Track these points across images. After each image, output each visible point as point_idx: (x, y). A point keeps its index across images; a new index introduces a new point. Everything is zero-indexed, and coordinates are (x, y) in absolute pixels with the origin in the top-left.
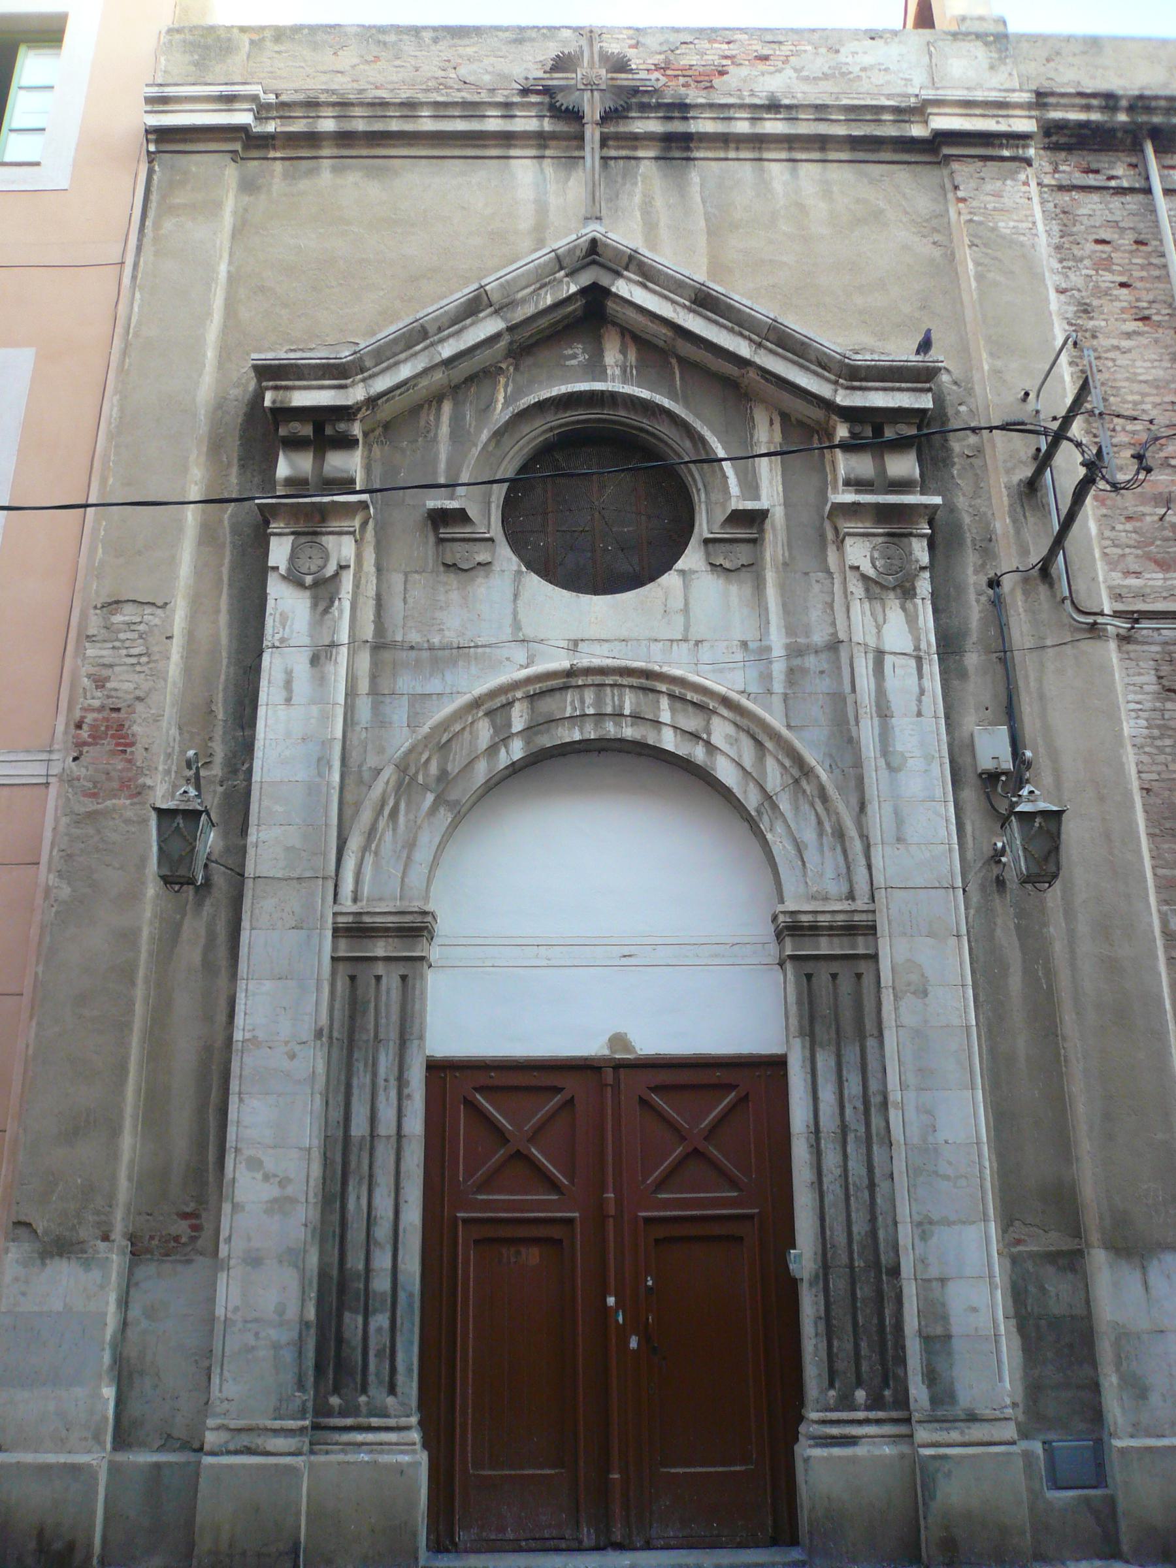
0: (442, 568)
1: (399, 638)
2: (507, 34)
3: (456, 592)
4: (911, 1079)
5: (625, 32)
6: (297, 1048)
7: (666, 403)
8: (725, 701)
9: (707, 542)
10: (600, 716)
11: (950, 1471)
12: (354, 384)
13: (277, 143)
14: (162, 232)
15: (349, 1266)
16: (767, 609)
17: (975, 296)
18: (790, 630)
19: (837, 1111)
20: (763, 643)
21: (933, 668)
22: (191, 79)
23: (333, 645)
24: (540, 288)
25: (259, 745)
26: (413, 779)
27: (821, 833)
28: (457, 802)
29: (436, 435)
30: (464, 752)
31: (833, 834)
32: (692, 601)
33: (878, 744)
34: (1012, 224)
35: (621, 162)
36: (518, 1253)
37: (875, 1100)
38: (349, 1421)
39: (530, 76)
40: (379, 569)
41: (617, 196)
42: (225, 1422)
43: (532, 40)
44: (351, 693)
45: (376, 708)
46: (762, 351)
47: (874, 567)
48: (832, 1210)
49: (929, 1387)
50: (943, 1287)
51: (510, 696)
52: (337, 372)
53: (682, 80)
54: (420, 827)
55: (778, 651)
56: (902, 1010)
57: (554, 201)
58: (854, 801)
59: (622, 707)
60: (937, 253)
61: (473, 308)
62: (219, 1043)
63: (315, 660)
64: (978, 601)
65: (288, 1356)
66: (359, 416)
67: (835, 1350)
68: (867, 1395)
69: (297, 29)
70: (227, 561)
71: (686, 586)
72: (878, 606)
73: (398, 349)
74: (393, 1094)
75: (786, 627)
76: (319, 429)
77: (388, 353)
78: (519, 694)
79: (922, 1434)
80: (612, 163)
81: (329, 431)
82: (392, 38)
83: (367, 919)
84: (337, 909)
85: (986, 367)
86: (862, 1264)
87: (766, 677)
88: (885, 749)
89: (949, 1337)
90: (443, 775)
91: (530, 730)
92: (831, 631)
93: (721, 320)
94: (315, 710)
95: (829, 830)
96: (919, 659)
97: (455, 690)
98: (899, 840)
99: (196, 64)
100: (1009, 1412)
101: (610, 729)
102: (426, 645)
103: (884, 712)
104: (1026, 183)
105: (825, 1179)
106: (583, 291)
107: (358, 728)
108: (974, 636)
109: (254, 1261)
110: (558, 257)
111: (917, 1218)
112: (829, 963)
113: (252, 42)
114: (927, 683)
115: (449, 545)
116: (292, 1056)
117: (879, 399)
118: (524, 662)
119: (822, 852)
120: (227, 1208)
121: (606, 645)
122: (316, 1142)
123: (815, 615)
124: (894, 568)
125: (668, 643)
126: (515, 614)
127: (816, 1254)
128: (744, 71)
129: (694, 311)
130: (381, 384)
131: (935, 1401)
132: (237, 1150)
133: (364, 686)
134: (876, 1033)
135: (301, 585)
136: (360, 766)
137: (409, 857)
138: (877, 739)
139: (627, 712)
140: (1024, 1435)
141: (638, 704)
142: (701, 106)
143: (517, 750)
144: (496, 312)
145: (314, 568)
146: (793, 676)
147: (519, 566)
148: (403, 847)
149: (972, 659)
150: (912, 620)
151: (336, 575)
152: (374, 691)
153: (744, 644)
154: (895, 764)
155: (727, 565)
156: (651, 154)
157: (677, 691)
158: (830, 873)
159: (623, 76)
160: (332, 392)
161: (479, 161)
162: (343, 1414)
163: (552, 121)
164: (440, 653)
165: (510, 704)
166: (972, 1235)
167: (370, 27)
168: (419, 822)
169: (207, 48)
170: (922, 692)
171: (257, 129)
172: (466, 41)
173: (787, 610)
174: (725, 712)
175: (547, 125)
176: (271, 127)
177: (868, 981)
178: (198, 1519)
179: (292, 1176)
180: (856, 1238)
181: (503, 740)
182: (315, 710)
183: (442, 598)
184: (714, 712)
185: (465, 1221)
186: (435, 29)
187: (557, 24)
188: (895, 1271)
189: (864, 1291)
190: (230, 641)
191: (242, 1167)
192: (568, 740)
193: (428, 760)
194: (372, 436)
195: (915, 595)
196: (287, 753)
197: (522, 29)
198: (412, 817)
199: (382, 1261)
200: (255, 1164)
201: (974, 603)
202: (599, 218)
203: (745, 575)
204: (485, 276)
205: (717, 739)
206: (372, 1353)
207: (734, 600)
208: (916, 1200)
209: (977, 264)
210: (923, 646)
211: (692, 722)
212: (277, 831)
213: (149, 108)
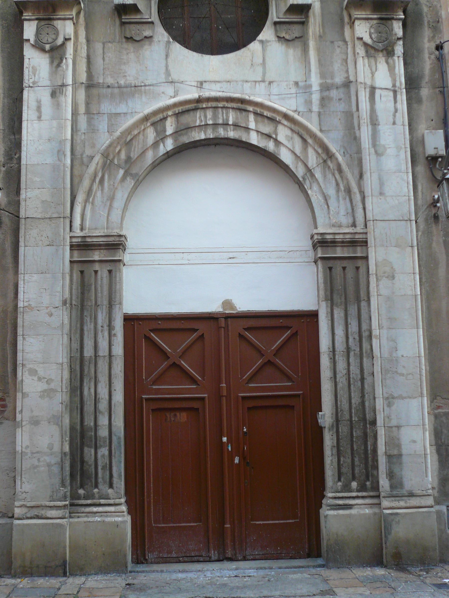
0: (124, 40)
1: (101, 81)
3: (133, 54)
4: (385, 323)
6: (53, 310)
8: (286, 116)
9: (276, 23)
10: (215, 125)
11: (399, 521)
15: (86, 424)
16: (309, 63)
18: (323, 75)
19: (344, 340)
20: (307, 83)
21: (403, 97)
23: (64, 85)
25: (24, 143)
26: (112, 161)
27: (338, 190)
28: (137, 174)
30: (140, 146)
31: (345, 190)
32: (267, 59)
33: (370, 141)
36: (175, 415)
37: (365, 334)
38: (89, 502)
40: (88, 41)
42: (25, 503)
44: (75, 113)
45: (89, 122)
47: (371, 38)
48: (341, 392)
49: (390, 480)
50: (398, 430)
51: (165, 114)
54: (116, 188)
55: (316, 87)
56: (381, 286)
58: (356, 172)
59: (228, 120)
62: (10, 308)
63: (53, 94)
64: (429, 58)
65: (56, 469)
67: (342, 463)
68: (358, 485)
71: (264, 50)
72: (372, 61)
74: (106, 334)
75: (320, 74)
78: (170, 113)
79: (385, 503)
83: (89, 240)
84: (72, 234)
86: (357, 419)
87: (309, 102)
88: (374, 144)
89: (400, 456)
90: (128, 159)
91: (177, 133)
92: (346, 75)
94: (55, 123)
95: (342, 188)
96: (395, 92)
97: (134, 110)
98: (381, 194)
100: (430, 492)
101: (221, 132)
102: (116, 85)
103: (374, 122)
105: (338, 376)
107: (80, 133)
108: (427, 78)
109: (35, 422)
111: (386, 395)
112: (342, 260)
114: (399, 106)
115: (127, 26)
116: (51, 315)
118: (172, 94)
119: (339, 201)
120: (19, 395)
121: (218, 85)
122: (65, 360)
123: (337, 66)
124: (382, 38)
125: (254, 83)
126: (167, 66)
127: (332, 414)
131: (392, 487)
132: (23, 365)
133: (82, 109)
134: (366, 299)
135: (43, 50)
136: (82, 155)
137: (111, 205)
138: (370, 138)
139: (231, 123)
140: (437, 502)
141: (237, 118)
143: (169, 145)
145: (50, 40)
146: (324, 101)
147: (168, 38)
148: (107, 200)
149: (425, 92)
150: (391, 69)
151: (63, 44)
152: (88, 112)
153: (296, 83)
154: (380, 152)
155: (287, 37)
157: (259, 110)
158: (342, 212)
162: (86, 498)
164: (125, 90)
165: (165, 119)
166: (414, 404)
168: (116, 185)
170: (396, 111)
173: (321, 63)
174: (285, 123)
177: (362, 270)
178: (14, 551)
179: (53, 378)
180: (354, 406)
181: (162, 139)
182: (55, 123)
183: (125, 57)
184: (279, 122)
185: (147, 399)
188: (374, 423)
189: (357, 433)
190: (4, 84)
191: (26, 374)
192: (198, 139)
193: (120, 151)
195: (394, 55)
196: (40, 148)
198: (112, 183)
199: (103, 421)
200: (33, 372)
201: (427, 59)
203: (298, 43)
205: (281, 138)
206: (100, 468)
207: (291, 58)
208: (385, 386)
210: (398, 84)
211: (267, 128)
212: (37, 192)
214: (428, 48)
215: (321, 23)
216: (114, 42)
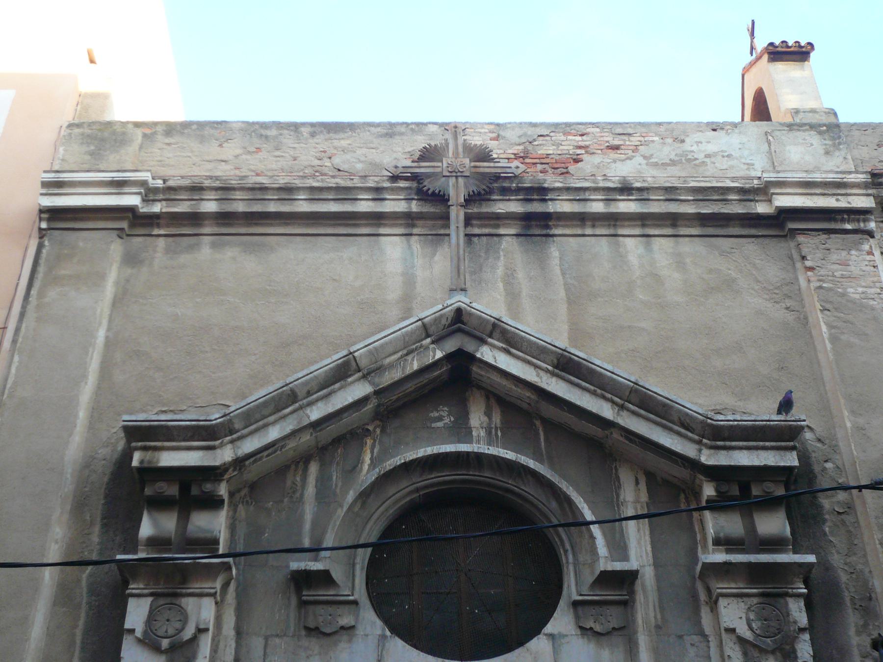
0: (303, 633)
2: (379, 129)
3: (317, 657)
5: (486, 127)
7: (531, 464)
9: (576, 604)
12: (222, 445)
13: (162, 221)
14: (47, 300)
17: (831, 357)
22: (86, 167)
24: (407, 354)
29: (302, 495)
34: (860, 290)
35: (484, 239)
39: (400, 165)
40: (239, 633)
41: (481, 270)
43: (402, 134)
46: (625, 413)
47: (751, 628)
52: (206, 434)
53: (539, 167)
57: (421, 274)
60: (790, 317)
61: (343, 372)
66: (226, 477)
69: (186, 125)
70: (81, 623)
71: (556, 651)
73: (266, 412)
76: (185, 488)
77: (258, 416)
80: (475, 239)
81: (195, 491)
82: (273, 132)
85: (849, 425)
93: (584, 384)
99: (92, 154)
104: (870, 253)
106: (449, 357)
110: (424, 325)
113: (145, 136)
115: (311, 608)
117: (744, 458)
128: (597, 159)
129: (557, 376)
130: (250, 445)
135: (156, 648)
144: (364, 377)
145: (171, 631)
147: (383, 630)
151: (194, 639)
155: (598, 628)
159: (486, 164)
160: (200, 454)
167: (253, 123)
169: (103, 140)
171: (144, 209)
172: (342, 135)
175: (415, 207)
176: (157, 208)
186: (312, 125)
187: (425, 121)
194: (237, 496)
197: (392, 125)
202: (463, 290)
204: (355, 343)
209: (830, 326)
213: (44, 191)
214: (859, 645)
215: (657, 604)
216: (285, 635)
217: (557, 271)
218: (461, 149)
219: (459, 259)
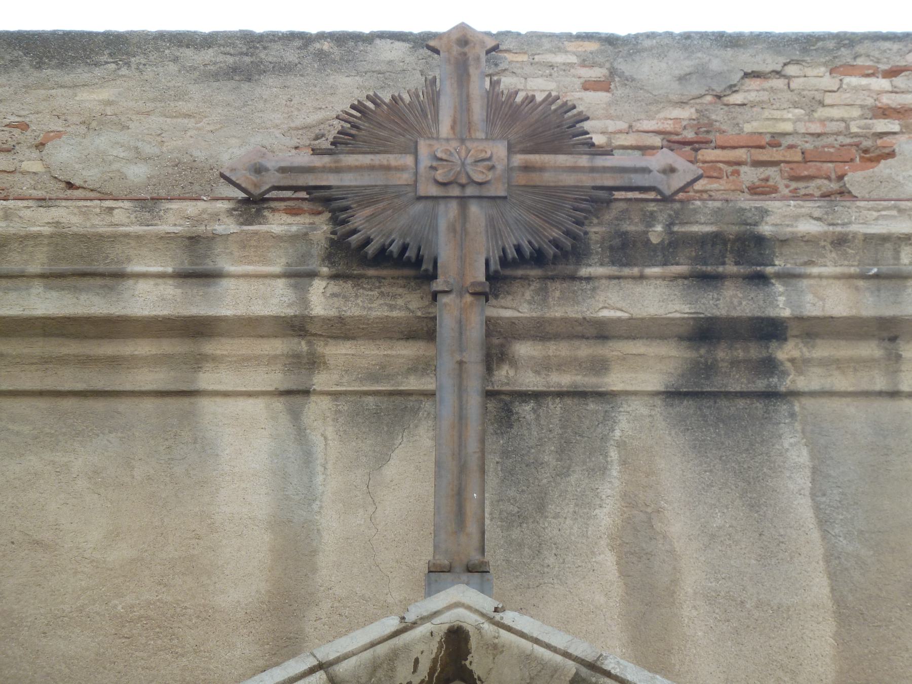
2: (208, 55)
5: (571, 46)
35: (555, 407)
39: (271, 163)
41: (541, 508)
43: (284, 69)
53: (749, 175)
57: (332, 525)
80: (526, 410)
142: (809, 240)
156: (653, 381)
159: (562, 160)
161: (99, 405)
163: (334, 287)
172: (82, 74)
175: (321, 299)
187: (366, 28)
197: (252, 41)
202: (476, 570)
217: (804, 509)
218: (478, 110)
219: (462, 469)
